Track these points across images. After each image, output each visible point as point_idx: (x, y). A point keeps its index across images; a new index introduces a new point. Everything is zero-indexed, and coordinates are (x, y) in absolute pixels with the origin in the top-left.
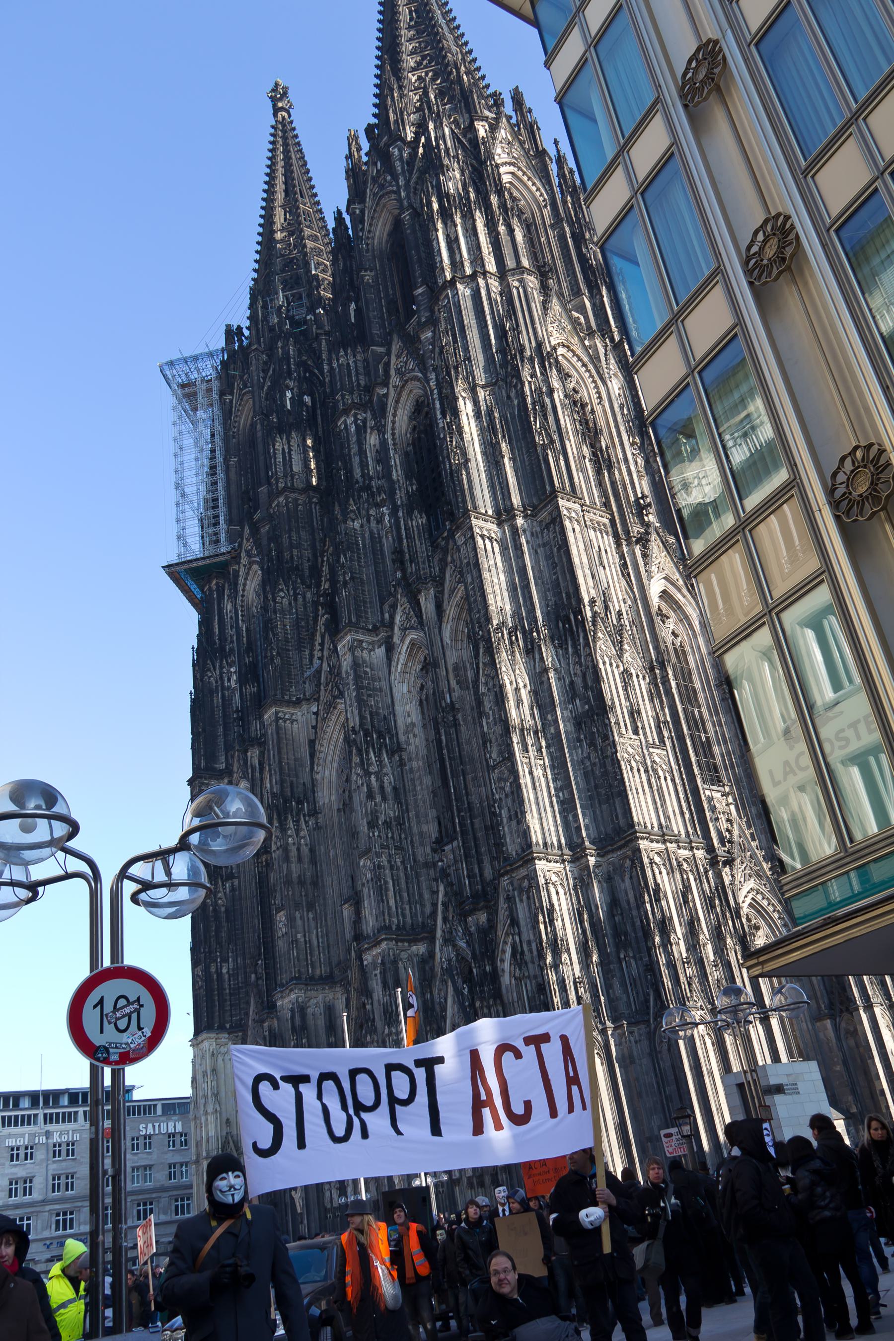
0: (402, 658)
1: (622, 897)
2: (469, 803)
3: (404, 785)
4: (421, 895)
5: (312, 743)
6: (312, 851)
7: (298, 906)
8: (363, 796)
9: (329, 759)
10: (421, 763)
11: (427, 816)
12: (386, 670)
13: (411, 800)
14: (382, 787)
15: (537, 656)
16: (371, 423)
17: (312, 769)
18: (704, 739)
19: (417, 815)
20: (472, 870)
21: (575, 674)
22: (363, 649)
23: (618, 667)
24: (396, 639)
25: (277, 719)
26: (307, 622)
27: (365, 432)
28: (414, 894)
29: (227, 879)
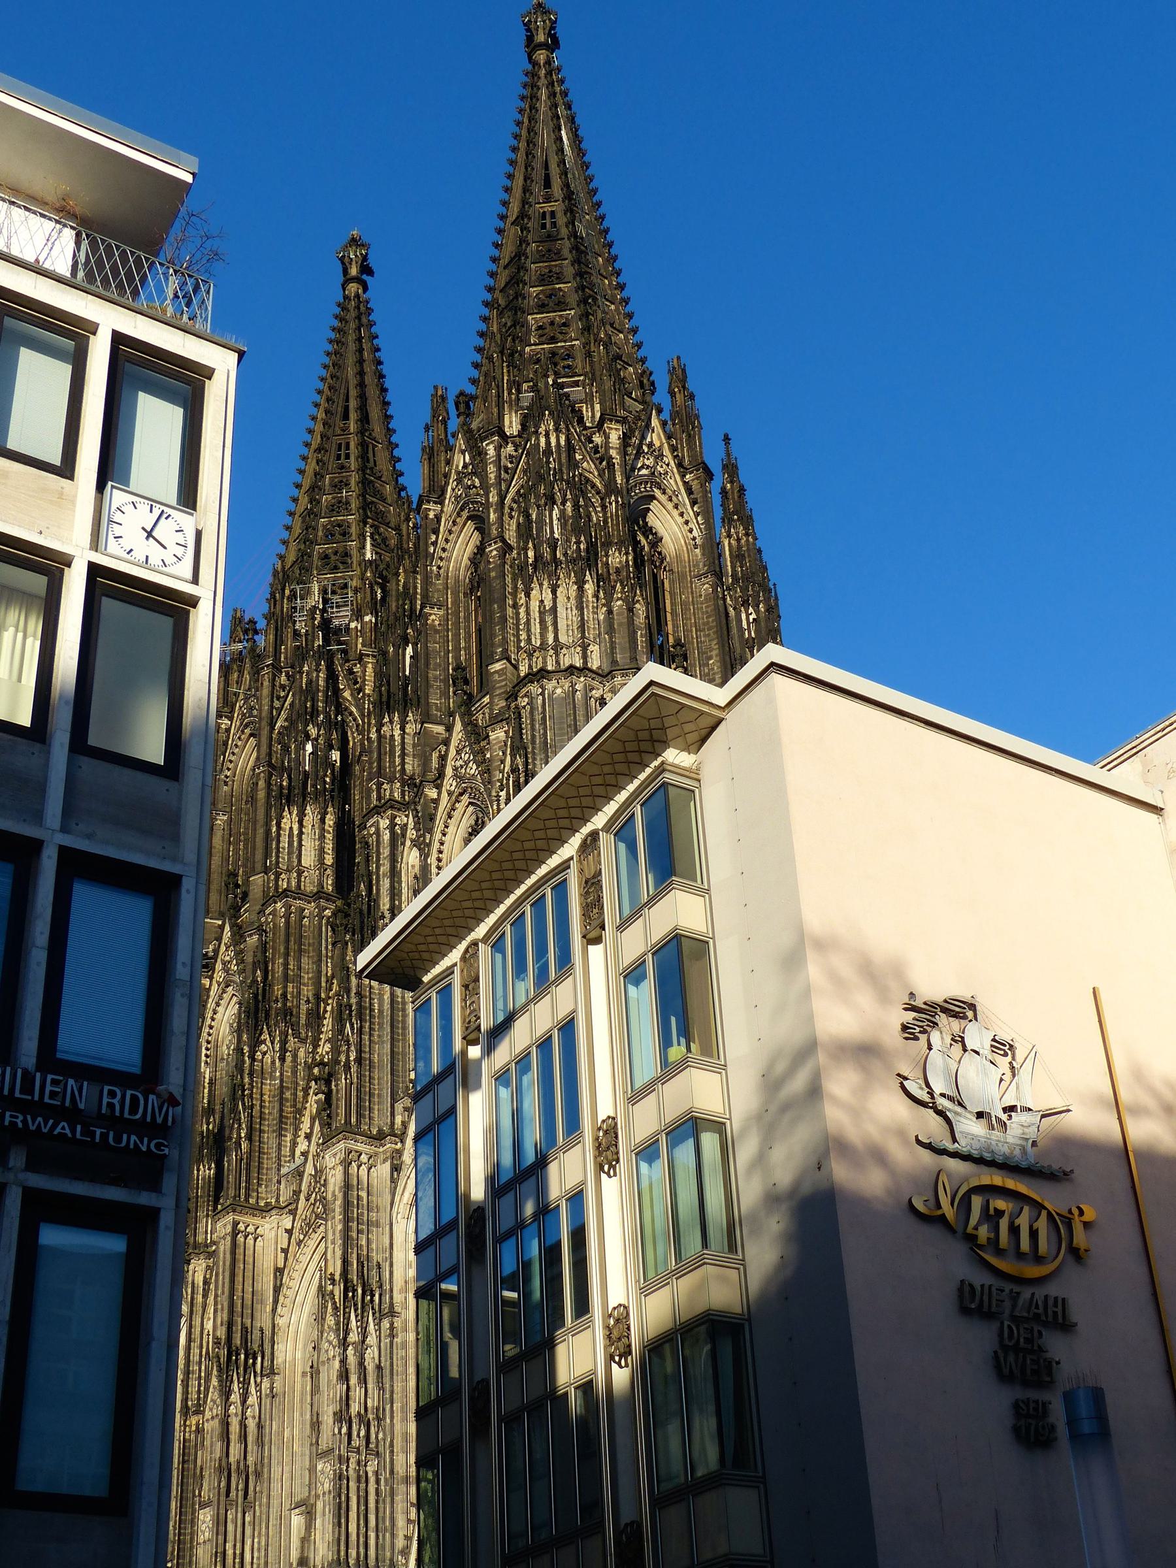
4: (393, 1519)
5: (279, 1272)
8: (334, 1375)
9: (299, 1299)
12: (388, 1198)
14: (361, 1364)
16: (411, 833)
17: (274, 1310)
25: (235, 1233)
26: (295, 1094)
27: (403, 844)
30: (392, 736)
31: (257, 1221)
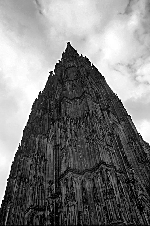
0: (50, 140)
1: (96, 185)
2: (58, 168)
3: (46, 168)
6: (25, 191)
7: (18, 205)
10: (51, 163)
11: (50, 176)
13: (47, 172)
14: (40, 168)
15: (77, 124)
18: (125, 156)
19: (48, 176)
20: (57, 186)
21: (87, 128)
22: (42, 138)
23: (99, 125)
24: (49, 136)
25: (24, 160)
27: (51, 101)
28: (43, 197)
29: (10, 203)
30: (50, 93)
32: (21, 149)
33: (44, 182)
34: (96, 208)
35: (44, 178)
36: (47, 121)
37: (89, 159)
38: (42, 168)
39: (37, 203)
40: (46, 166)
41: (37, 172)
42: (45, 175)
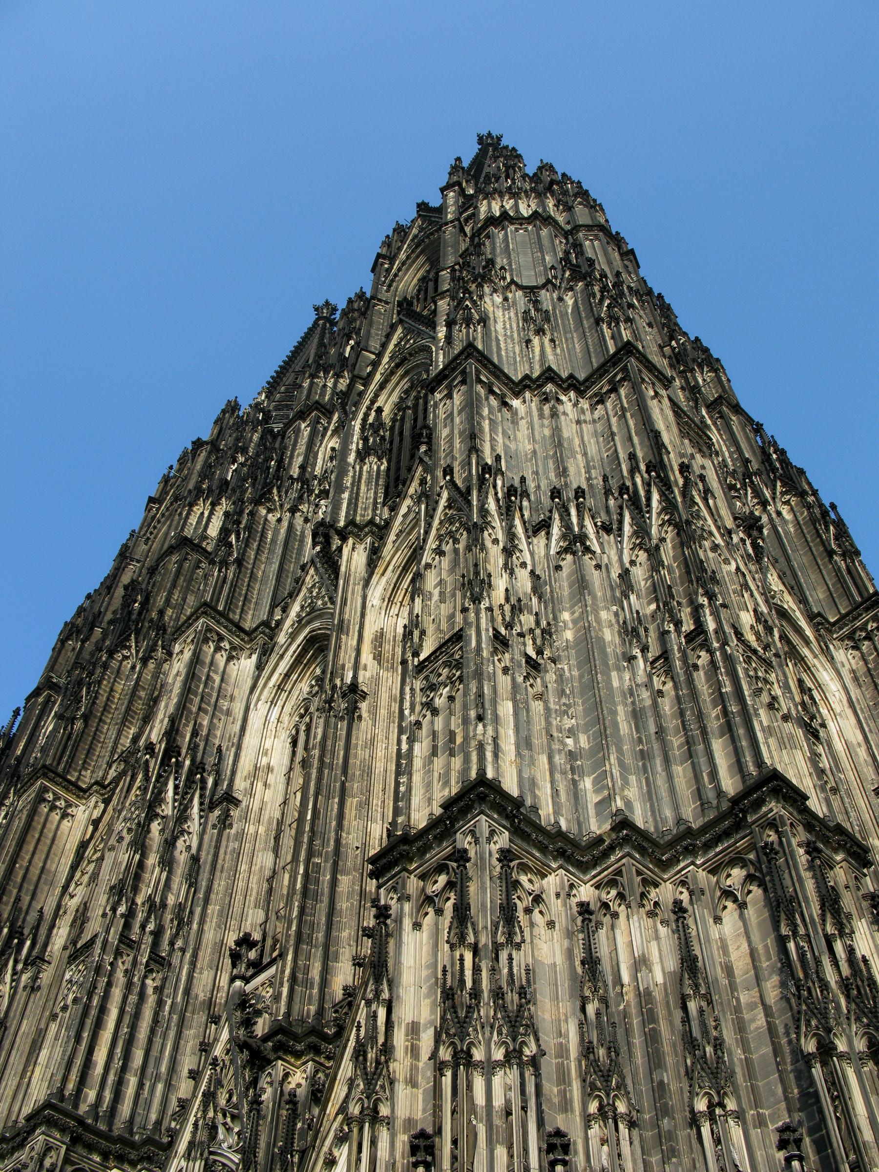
0: (283, 667)
2: (338, 842)
10: (262, 830)
13: (220, 885)
14: (170, 844)
17: (66, 887)
20: (307, 970)
22: (218, 649)
25: (40, 799)
27: (323, 436)
30: (325, 386)
31: (72, 799)
32: (19, 752)
33: (188, 955)
34: (706, 1130)
35: (190, 923)
36: (271, 551)
37: (644, 765)
38: (189, 848)
39: (108, 1095)
40: (224, 843)
41: (141, 865)
42: (207, 901)
